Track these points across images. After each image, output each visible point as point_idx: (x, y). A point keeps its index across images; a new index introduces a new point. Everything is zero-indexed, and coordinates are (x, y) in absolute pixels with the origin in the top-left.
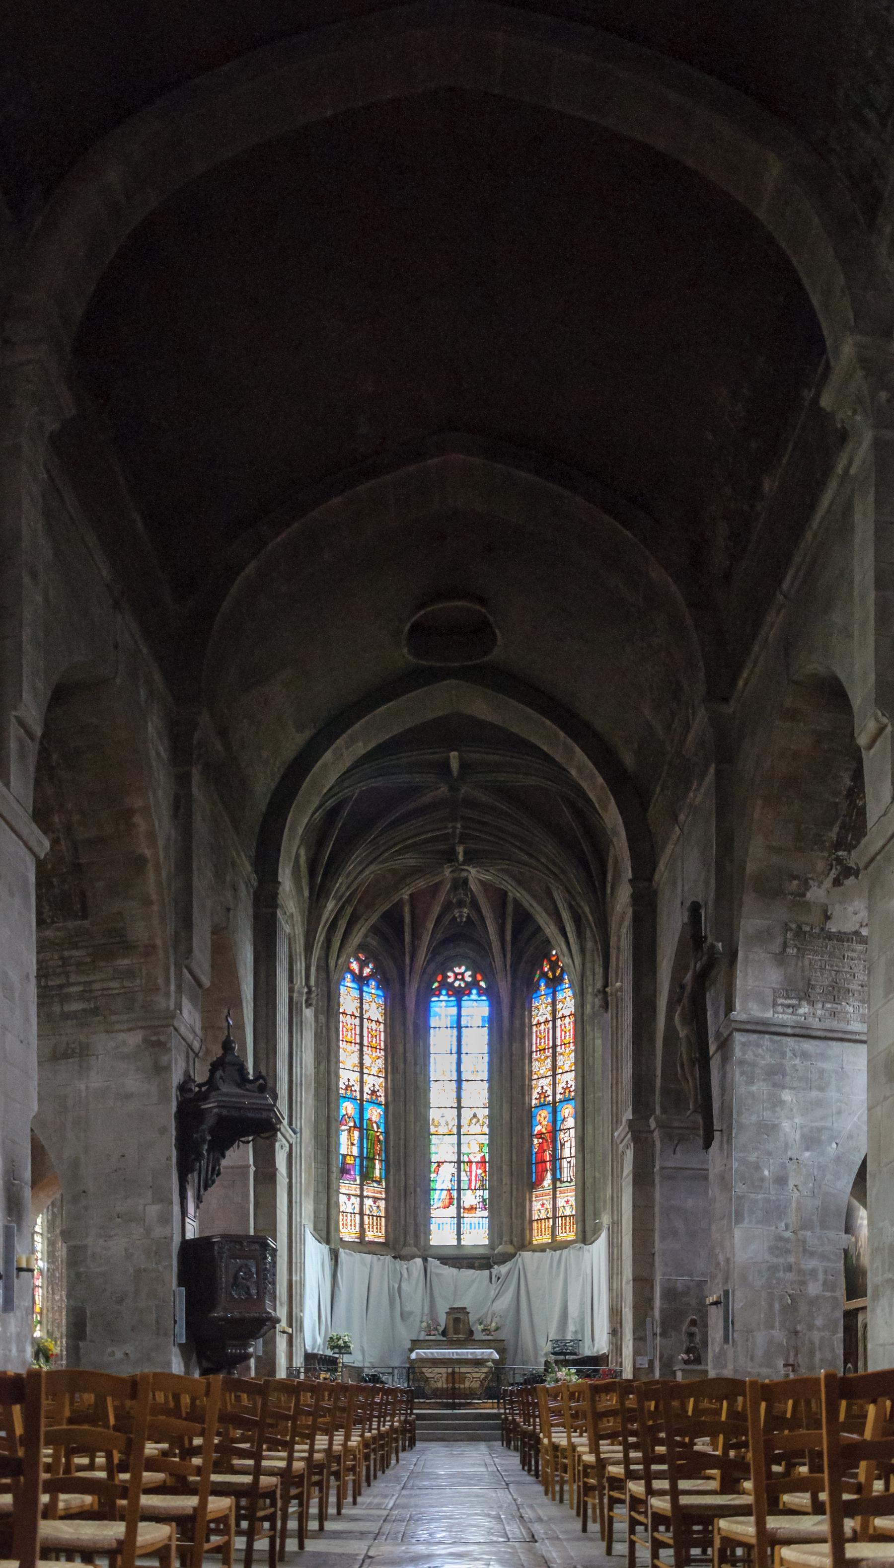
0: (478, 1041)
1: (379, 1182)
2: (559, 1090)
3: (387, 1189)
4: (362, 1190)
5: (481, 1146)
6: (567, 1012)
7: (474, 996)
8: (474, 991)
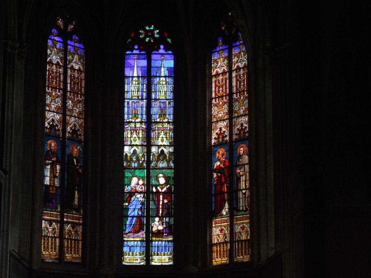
0: (164, 89)
1: (78, 210)
2: (235, 131)
3: (84, 217)
4: (62, 217)
5: (167, 178)
6: (241, 65)
7: (162, 51)
8: (162, 47)
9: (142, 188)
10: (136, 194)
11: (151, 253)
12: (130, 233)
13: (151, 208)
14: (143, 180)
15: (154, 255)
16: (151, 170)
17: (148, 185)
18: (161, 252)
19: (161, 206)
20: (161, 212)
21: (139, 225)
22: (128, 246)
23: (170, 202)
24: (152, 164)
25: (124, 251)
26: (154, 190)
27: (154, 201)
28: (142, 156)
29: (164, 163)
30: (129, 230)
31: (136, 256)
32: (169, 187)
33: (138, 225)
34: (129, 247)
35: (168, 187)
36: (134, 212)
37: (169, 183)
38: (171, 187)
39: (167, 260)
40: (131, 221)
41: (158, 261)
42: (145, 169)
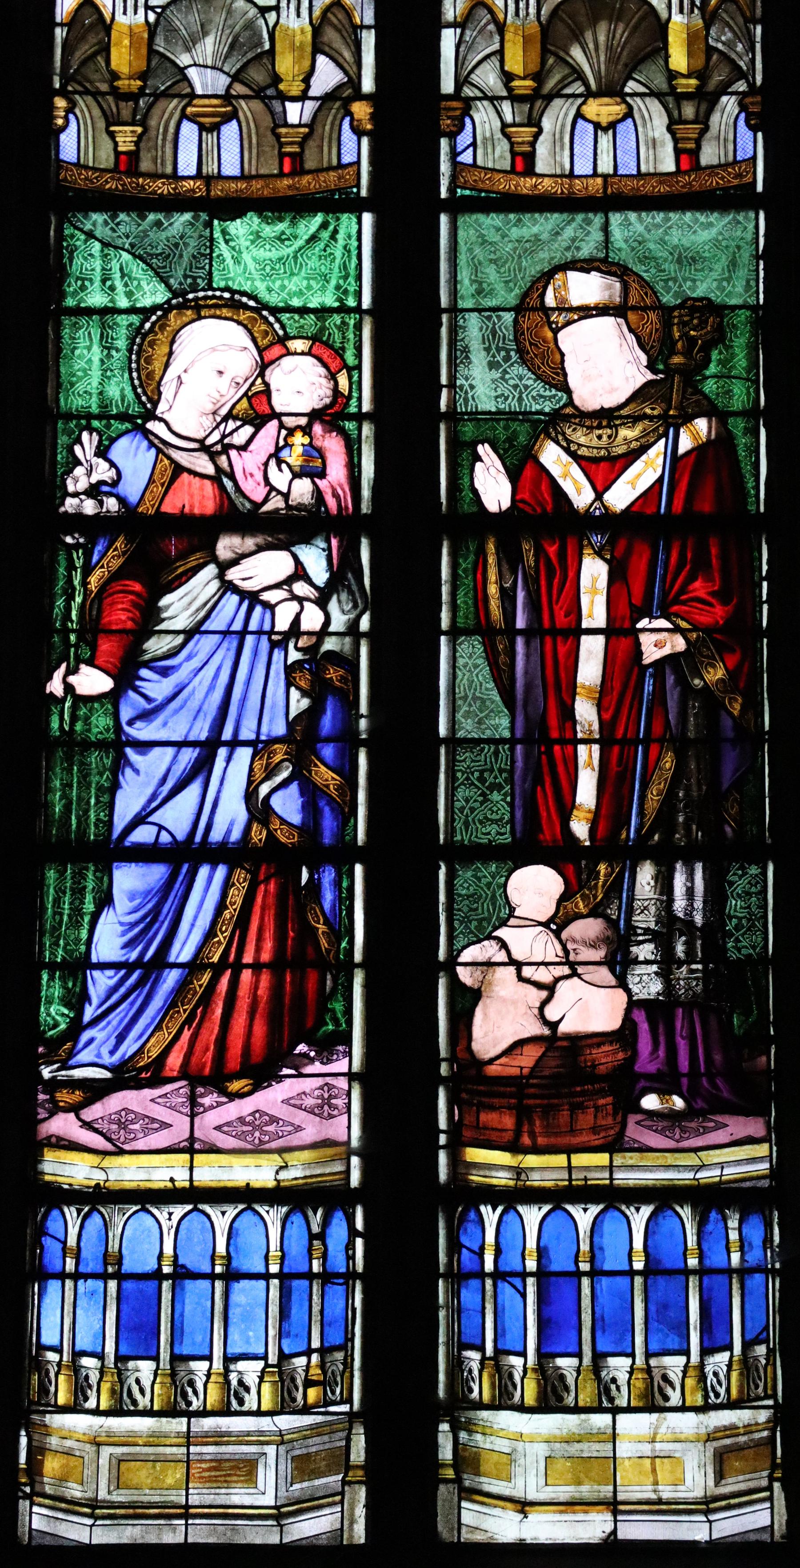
5: (676, 335)
9: (312, 468)
10: (226, 545)
11: (456, 1365)
12: (138, 1085)
13: (443, 731)
14: (329, 354)
15: (504, 1400)
16: (444, 219)
17: (407, 407)
18: (599, 1357)
19: (585, 712)
20: (586, 791)
21: (277, 966)
22: (112, 1268)
23: (722, 650)
24: (453, 136)
25: (49, 1337)
26: (493, 487)
27: (495, 639)
28: (317, 31)
29: (625, 129)
30: (129, 1047)
31: (225, 1411)
32: (700, 450)
33: (257, 967)
34: (120, 1277)
35: (685, 443)
36: (193, 792)
37: (710, 387)
38: (742, 441)
39: (695, 1479)
40: (155, 914)
41: (564, 1492)
42: (356, 206)
